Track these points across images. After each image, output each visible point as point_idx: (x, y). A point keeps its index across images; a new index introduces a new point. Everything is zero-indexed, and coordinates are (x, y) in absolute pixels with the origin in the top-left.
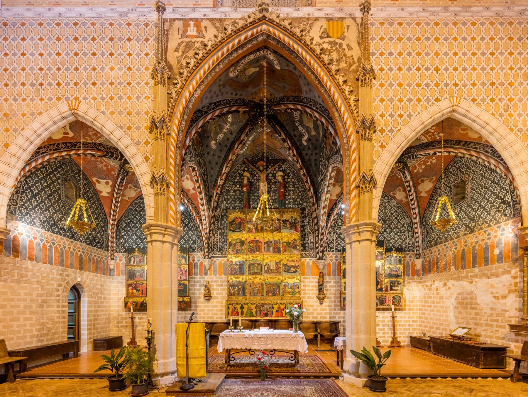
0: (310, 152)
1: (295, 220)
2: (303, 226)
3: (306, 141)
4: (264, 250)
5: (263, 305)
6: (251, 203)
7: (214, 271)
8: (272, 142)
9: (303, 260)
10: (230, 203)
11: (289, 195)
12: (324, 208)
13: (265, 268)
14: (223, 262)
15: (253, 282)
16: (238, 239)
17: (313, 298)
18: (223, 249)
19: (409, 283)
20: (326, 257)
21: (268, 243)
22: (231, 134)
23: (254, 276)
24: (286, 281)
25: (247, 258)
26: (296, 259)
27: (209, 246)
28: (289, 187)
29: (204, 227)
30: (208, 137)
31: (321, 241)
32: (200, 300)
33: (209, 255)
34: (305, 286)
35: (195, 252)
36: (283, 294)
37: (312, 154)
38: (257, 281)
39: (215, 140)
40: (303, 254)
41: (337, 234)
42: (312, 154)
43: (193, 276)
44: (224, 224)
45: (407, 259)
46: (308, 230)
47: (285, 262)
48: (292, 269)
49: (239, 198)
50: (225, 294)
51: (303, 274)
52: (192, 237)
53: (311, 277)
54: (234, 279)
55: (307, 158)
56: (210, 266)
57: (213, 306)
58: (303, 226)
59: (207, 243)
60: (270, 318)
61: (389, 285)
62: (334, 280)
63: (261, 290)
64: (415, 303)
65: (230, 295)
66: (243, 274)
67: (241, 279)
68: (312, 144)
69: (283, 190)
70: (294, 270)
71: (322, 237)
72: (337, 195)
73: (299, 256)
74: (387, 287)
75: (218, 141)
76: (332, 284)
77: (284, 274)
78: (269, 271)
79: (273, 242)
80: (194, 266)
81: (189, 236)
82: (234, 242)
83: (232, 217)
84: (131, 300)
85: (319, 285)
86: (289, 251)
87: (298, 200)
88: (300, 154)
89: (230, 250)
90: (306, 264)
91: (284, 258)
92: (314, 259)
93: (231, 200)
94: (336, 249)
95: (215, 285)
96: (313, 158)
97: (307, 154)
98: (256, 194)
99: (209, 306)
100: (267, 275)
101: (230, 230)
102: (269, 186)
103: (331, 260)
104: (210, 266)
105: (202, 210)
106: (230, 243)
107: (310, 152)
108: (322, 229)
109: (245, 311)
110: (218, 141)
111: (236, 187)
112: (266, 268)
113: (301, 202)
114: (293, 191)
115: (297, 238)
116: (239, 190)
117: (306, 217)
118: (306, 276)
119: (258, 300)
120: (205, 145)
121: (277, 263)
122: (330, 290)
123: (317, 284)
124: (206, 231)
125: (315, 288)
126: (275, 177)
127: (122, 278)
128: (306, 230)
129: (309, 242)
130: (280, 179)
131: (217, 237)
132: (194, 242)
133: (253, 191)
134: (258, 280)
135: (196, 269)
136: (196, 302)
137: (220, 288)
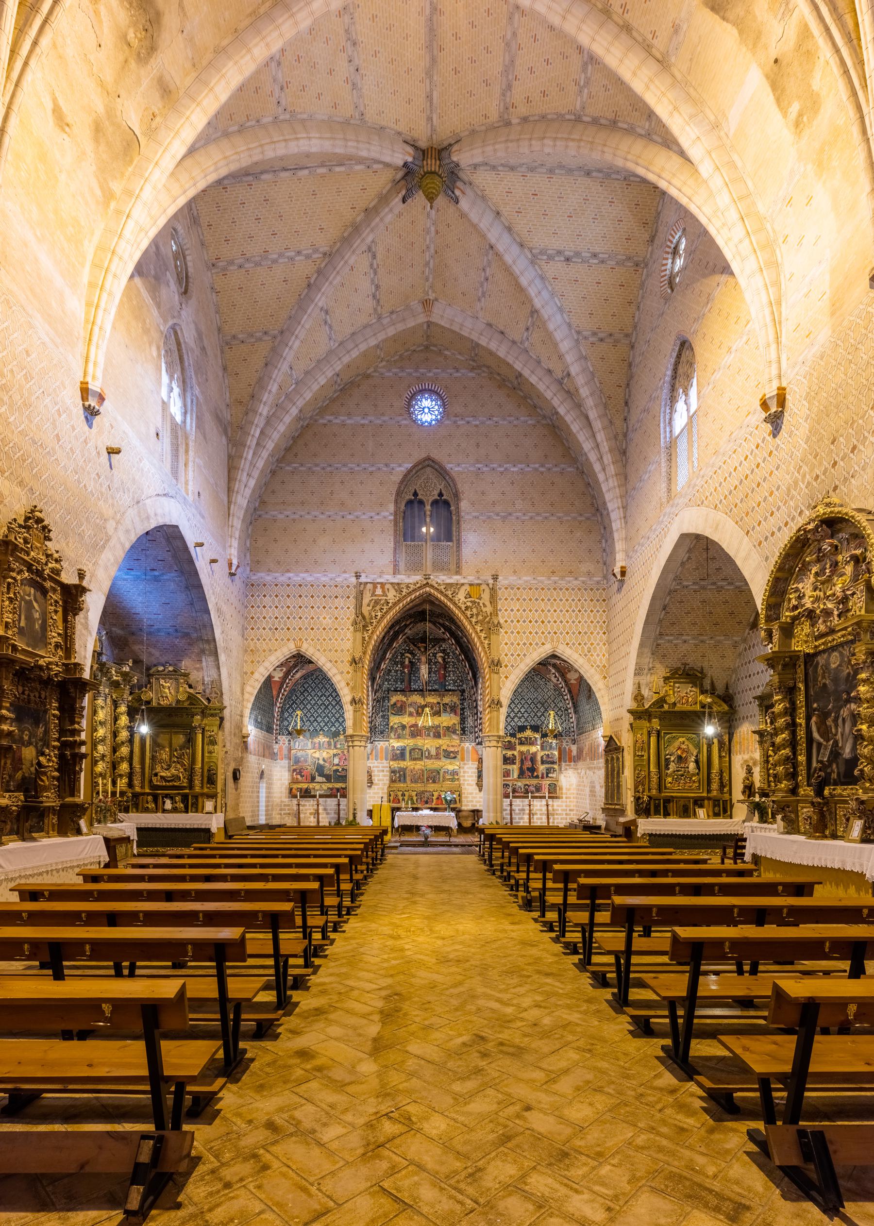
2: (462, 709)
5: (423, 792)
7: (376, 756)
9: (462, 744)
19: (566, 769)
21: (429, 729)
25: (408, 742)
34: (464, 772)
38: (418, 767)
45: (564, 744)
46: (467, 713)
50: (386, 780)
51: (463, 759)
53: (470, 762)
54: (395, 765)
57: (374, 793)
58: (462, 709)
61: (545, 772)
64: (572, 791)
65: (392, 781)
66: (404, 760)
67: (403, 764)
73: (458, 741)
74: (543, 774)
77: (443, 759)
78: (429, 757)
82: (396, 726)
83: (393, 700)
84: (295, 786)
86: (449, 736)
89: (392, 735)
91: (444, 743)
92: (473, 744)
109: (406, 798)
115: (456, 722)
119: (419, 787)
121: (437, 748)
126: (435, 657)
127: (285, 763)
130: (440, 660)
131: (379, 720)
134: (419, 765)
137: (381, 774)
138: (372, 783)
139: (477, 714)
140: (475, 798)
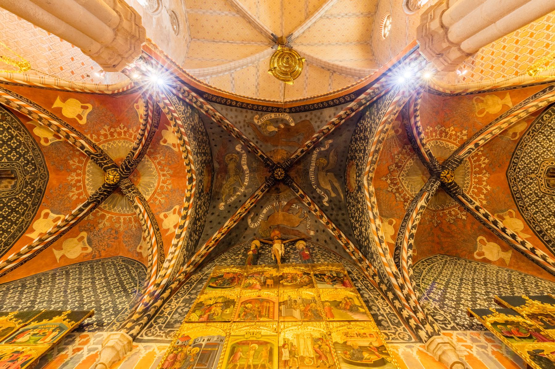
13: (280, 354)
16: (220, 297)
30: (218, 199)
31: (407, 300)
39: (226, 201)
47: (337, 338)
59: (146, 304)
68: (335, 205)
71: (406, 291)
72: (393, 237)
79: (299, 301)
106: (200, 305)
108: (396, 277)
112: (286, 355)
120: (212, 206)
129: (382, 312)
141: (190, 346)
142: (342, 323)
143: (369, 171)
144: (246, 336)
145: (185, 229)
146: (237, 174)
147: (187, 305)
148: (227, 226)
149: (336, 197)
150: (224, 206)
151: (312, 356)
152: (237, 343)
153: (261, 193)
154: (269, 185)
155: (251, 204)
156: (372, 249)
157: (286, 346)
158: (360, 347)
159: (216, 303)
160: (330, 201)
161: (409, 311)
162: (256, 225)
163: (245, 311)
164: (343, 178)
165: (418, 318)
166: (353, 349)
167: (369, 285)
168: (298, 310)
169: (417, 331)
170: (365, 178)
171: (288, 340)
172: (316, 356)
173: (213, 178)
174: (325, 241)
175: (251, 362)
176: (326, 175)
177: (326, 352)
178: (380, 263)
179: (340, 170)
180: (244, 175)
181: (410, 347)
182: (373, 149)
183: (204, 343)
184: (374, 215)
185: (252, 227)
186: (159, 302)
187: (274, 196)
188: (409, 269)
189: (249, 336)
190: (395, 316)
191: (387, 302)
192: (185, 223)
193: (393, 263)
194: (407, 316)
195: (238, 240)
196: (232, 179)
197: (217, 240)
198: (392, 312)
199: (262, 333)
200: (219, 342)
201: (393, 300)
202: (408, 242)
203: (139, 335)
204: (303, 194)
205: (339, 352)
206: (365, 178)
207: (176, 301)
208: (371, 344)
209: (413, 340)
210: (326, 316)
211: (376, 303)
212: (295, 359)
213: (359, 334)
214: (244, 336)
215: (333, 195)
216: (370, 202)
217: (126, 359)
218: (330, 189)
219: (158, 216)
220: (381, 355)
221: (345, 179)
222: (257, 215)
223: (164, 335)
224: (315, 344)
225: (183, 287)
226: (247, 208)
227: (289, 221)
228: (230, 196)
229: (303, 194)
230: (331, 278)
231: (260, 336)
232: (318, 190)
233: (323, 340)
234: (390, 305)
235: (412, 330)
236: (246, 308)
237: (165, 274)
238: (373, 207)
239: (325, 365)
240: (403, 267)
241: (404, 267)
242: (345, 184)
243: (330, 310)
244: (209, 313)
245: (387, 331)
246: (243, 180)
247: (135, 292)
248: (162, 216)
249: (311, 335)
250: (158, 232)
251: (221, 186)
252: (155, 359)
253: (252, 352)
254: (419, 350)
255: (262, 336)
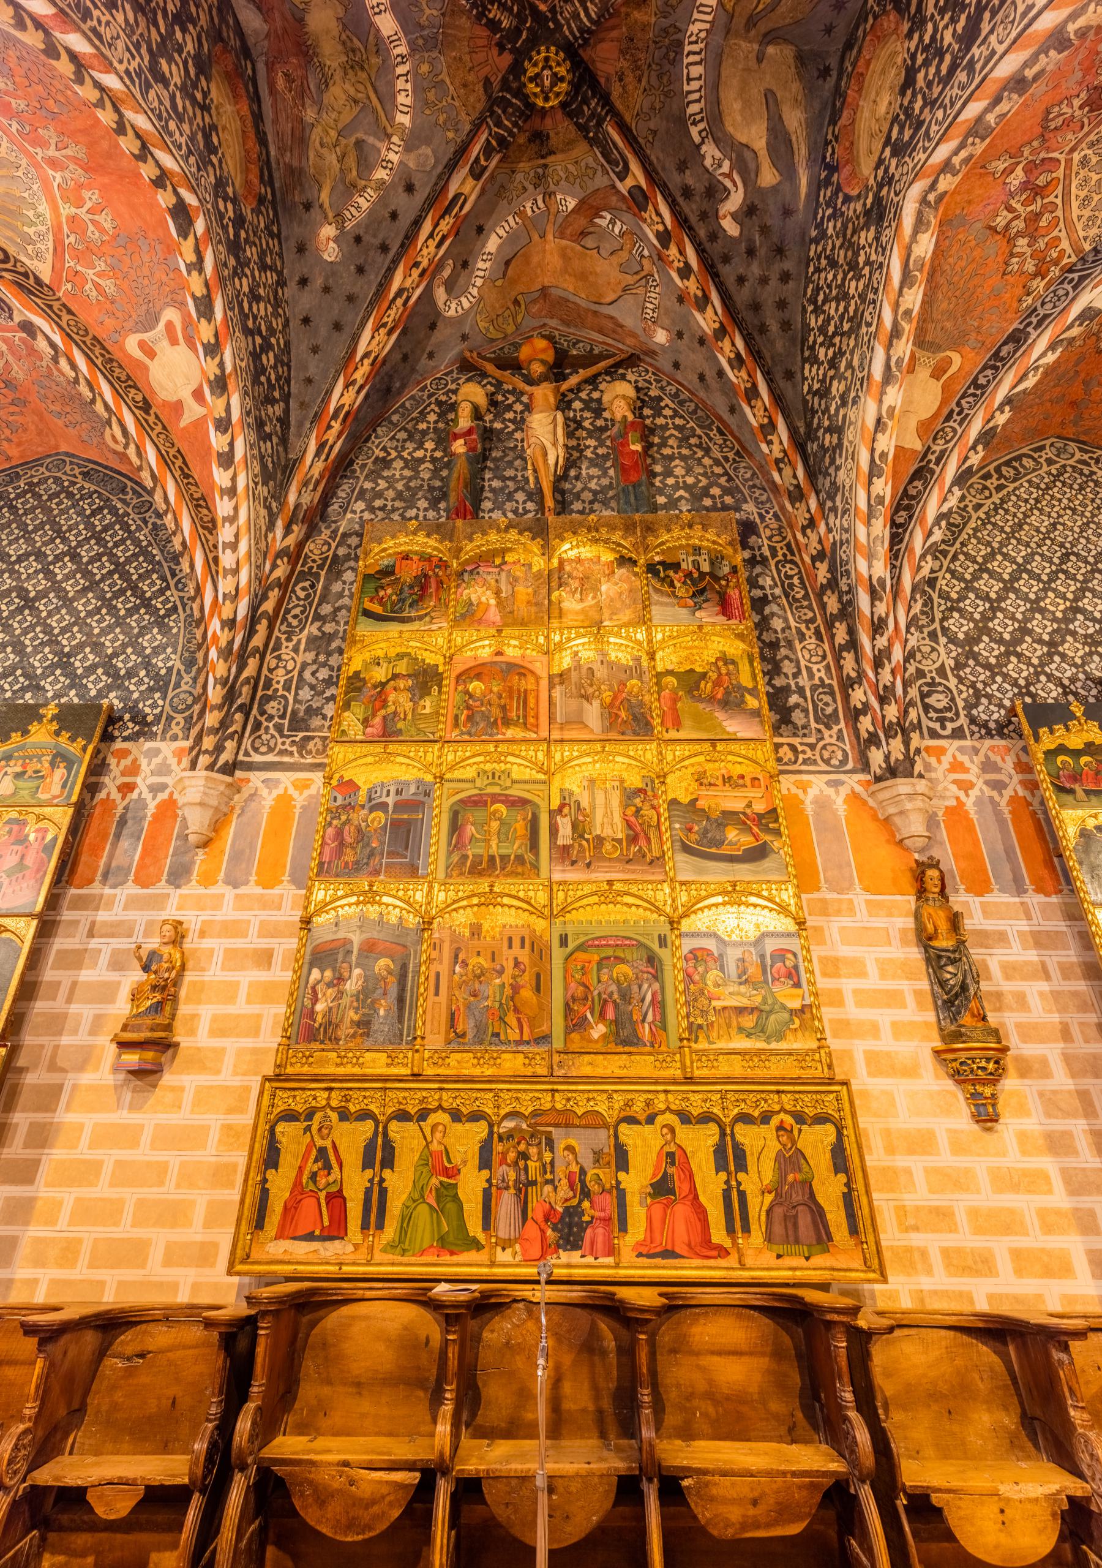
0: (755, 270)
1: (716, 560)
3: (734, 216)
4: (551, 719)
6: (487, 505)
7: (237, 857)
8: (582, 276)
10: (382, 508)
11: (668, 473)
12: (874, 471)
14: (300, 799)
15: (476, 931)
16: (400, 656)
17: (910, 1071)
18: (316, 722)
20: (928, 767)
22: (410, 188)
23: (484, 885)
24: (698, 922)
26: (746, 769)
27: (230, 696)
28: (664, 444)
29: (226, 585)
30: (308, 206)
31: (878, 664)
32: (87, 1078)
33: (219, 749)
35: (153, 736)
36: (694, 1030)
37: (764, 281)
39: (339, 219)
40: (786, 753)
41: (953, 640)
42: (764, 281)
43: (95, 889)
44: (341, 595)
48: (732, 834)
49: (431, 489)
52: (158, 662)
53: (860, 898)
55: (742, 296)
56: (218, 824)
57: (168, 1138)
58: (759, 604)
60: (599, 1268)
62: (1023, 925)
63: (527, 994)
66: (412, 871)
68: (764, 230)
69: (637, 447)
70: (747, 841)
71: (882, 642)
72: (924, 428)
73: (764, 753)
75: (349, 225)
76: (1020, 953)
77: (684, 866)
80: (122, 822)
81: (139, 651)
82: (380, 674)
85: (935, 960)
87: (715, 491)
88: (710, 267)
89: (352, 722)
90: (809, 808)
92: (854, 782)
93: (391, 494)
94: (973, 721)
95: (218, 957)
96: (770, 294)
97: (741, 280)
98: (509, 473)
99: (129, 1136)
100: (572, 876)
101: (367, 613)
102: (573, 443)
103: (966, 786)
104: (218, 824)
105: (223, 492)
106: (356, 682)
107: (755, 270)
108: (874, 595)
110: (349, 225)
111: (420, 446)
113: (728, 500)
114: (683, 458)
116: (433, 460)
117: (764, 561)
118: (826, 894)
121: (630, 795)
122: (1021, 1001)
123: (915, 954)
124: (227, 612)
125: (905, 986)
128: (777, 624)
132: (161, 684)
133: (495, 460)
135: (125, 844)
136: (50, 1097)
138: (165, 1046)
139: (847, 612)
140: (959, 1181)
141: (363, 807)
142: (697, 747)
143: (946, 167)
144: (478, 783)
145: (237, 429)
146: (355, 64)
147: (322, 658)
148: (366, 355)
149: (775, 189)
150: (336, 240)
151: (620, 836)
152: (461, 801)
153: (471, 182)
154: (501, 141)
155: (438, 246)
156: (842, 474)
157: (566, 810)
158: (724, 813)
159: (395, 677)
160: (749, 211)
161: (869, 693)
162: (466, 305)
163: (468, 707)
164: (831, 81)
165: (884, 717)
166: (708, 819)
167: (796, 581)
168: (596, 703)
169: (868, 747)
170: (916, 190)
171: (571, 794)
172: (628, 836)
173: (256, 98)
174: (702, 378)
175: (494, 850)
176: (760, 59)
177: (649, 826)
178: (847, 531)
179: (829, 30)
180: (386, 68)
181: (835, 784)
182: (1005, 69)
183: (390, 801)
184: (888, 367)
185: (452, 313)
186: (252, 663)
187: (525, 169)
188: (923, 557)
189: (486, 782)
190: (832, 694)
191: (826, 646)
192: (228, 404)
193: (882, 550)
194: (859, 706)
195: (413, 370)
196: (338, 92)
197: (348, 413)
198: (827, 681)
199: (514, 776)
200: (421, 798)
201: (842, 648)
202: (966, 458)
203: (241, 753)
204: (643, 183)
205: (677, 826)
206: (916, 190)
207: (291, 645)
208: (749, 805)
209: (850, 766)
210: (662, 724)
211: (795, 653)
212: (584, 843)
213: (730, 778)
214: (473, 781)
215: (768, 177)
216: (896, 306)
217: (237, 811)
218: (760, 144)
219: (123, 349)
220: (762, 835)
221: (839, 93)
222: (465, 265)
223: (294, 749)
224: (627, 806)
225: (293, 591)
226: (425, 263)
227: (582, 276)
228: (351, 189)
229: (643, 183)
230: (694, 583)
231: (509, 783)
232: (710, 151)
233: (645, 792)
234: (829, 658)
235: (858, 737)
236: (471, 696)
237: (237, 589)
238: (896, 332)
239: (644, 856)
240: (909, 549)
241: (912, 551)
242: (833, 122)
243: (675, 700)
244: (383, 712)
245: (796, 741)
246: (388, 99)
247: (175, 609)
248: (131, 345)
249: (622, 781)
250: (152, 419)
251: (301, 139)
252: (297, 811)
253: (495, 825)
254: (853, 792)
255: (513, 782)
